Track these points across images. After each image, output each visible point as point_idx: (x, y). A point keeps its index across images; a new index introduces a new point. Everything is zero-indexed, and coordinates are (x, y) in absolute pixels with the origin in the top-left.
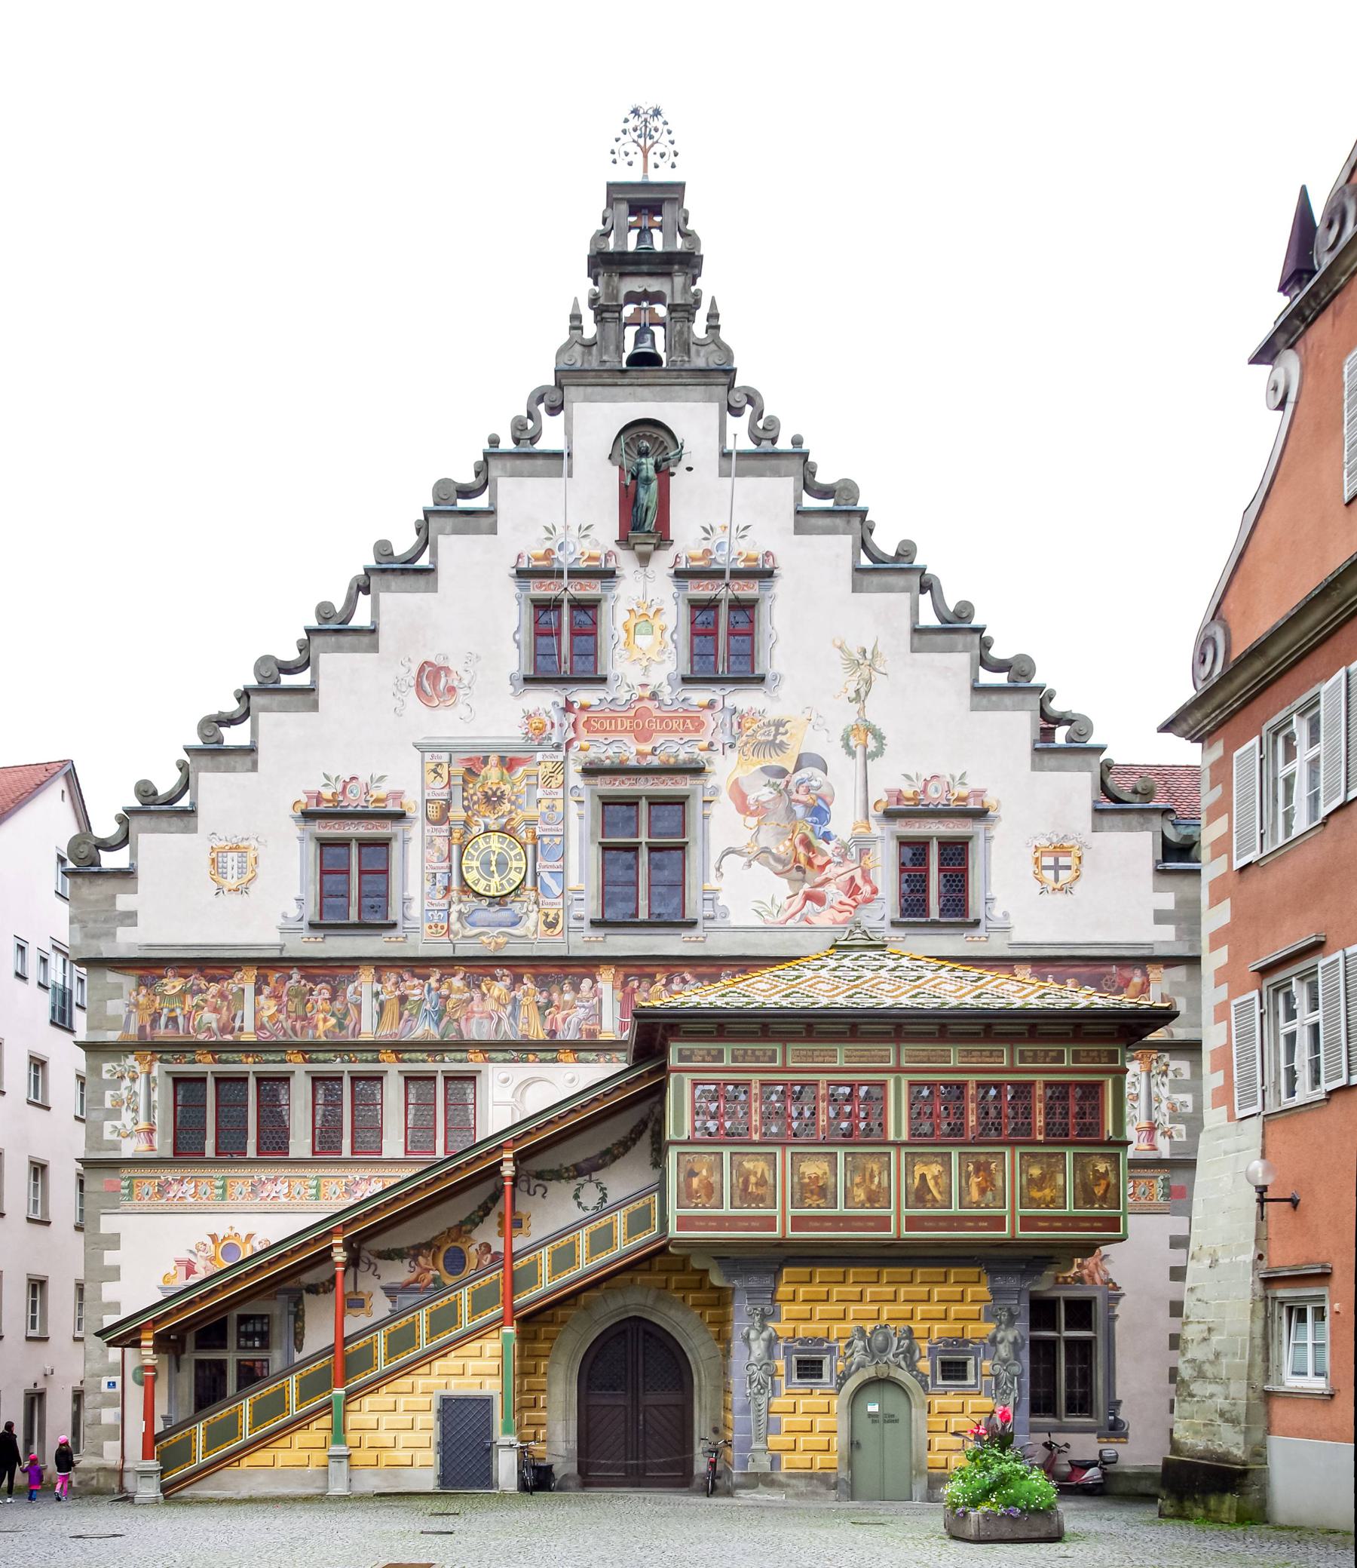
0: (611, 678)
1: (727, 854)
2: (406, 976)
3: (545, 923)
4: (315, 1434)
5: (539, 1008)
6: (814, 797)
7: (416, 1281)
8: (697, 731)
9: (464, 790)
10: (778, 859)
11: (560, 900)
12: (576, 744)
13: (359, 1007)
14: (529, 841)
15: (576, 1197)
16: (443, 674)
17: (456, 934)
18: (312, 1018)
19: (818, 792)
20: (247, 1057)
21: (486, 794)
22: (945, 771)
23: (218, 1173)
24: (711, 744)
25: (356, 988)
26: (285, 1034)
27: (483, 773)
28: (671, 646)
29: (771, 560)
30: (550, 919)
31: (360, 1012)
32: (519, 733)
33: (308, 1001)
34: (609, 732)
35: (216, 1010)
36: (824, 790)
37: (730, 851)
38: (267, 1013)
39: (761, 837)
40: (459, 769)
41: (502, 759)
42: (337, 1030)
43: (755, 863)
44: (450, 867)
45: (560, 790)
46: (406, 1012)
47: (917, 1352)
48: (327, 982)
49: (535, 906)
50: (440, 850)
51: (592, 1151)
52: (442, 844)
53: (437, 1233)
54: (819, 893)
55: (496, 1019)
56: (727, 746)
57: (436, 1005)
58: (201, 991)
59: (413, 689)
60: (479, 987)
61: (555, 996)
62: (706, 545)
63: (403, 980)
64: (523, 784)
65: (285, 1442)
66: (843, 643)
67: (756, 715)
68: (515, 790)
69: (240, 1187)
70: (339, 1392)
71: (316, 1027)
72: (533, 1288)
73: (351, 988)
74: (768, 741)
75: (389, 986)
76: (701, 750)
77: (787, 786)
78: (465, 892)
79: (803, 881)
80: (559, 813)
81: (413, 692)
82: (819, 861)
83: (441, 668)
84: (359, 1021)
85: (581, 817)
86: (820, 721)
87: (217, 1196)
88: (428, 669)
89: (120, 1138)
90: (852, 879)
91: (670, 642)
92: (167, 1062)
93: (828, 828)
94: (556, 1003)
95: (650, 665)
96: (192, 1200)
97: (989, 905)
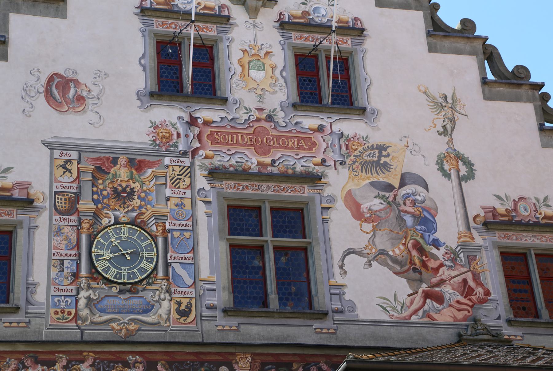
0: (230, 100)
1: (349, 254)
2: (28, 363)
3: (178, 311)
6: (419, 209)
8: (311, 149)
9: (93, 185)
10: (395, 261)
11: (192, 290)
12: (201, 152)
14: (160, 234)
16: (72, 86)
19: (423, 205)
21: (115, 190)
22: (530, 194)
24: (324, 161)
27: (112, 171)
28: (281, 81)
29: (359, 24)
30: (183, 307)
32: (147, 139)
34: (231, 144)
36: (428, 204)
37: (350, 252)
39: (377, 240)
40: (89, 167)
41: (131, 161)
43: (375, 264)
44: (79, 255)
45: (188, 192)
49: (167, 295)
50: (68, 238)
54: (436, 292)
56: (338, 163)
59: (42, 96)
62: (303, 8)
64: (152, 183)
66: (427, 89)
67: (360, 140)
68: (145, 188)
74: (373, 161)
76: (315, 165)
77: (395, 198)
78: (95, 280)
79: (421, 281)
80: (187, 210)
81: (42, 98)
82: (432, 264)
83: (72, 80)
85: (209, 215)
86: (417, 148)
88: (57, 80)
90: (465, 281)
91: (280, 78)
93: (437, 235)
95: (264, 94)
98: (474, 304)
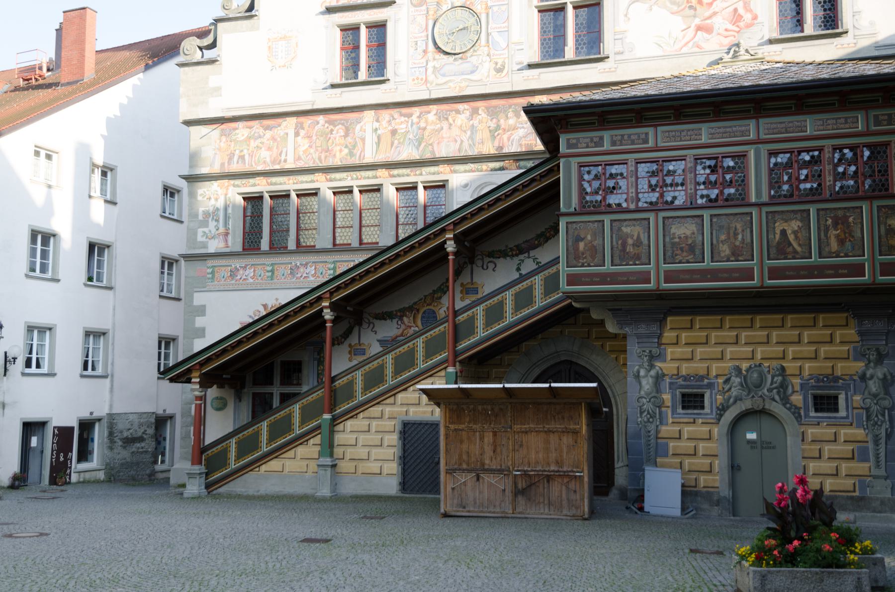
2: (396, 116)
4: (310, 449)
5: (490, 131)
7: (402, 335)
11: (506, 51)
13: (363, 140)
14: (483, 11)
15: (518, 269)
17: (431, 84)
18: (332, 150)
20: (289, 180)
23: (269, 260)
25: (361, 127)
26: (314, 163)
30: (499, 66)
31: (364, 144)
33: (330, 138)
35: (269, 149)
38: (302, 149)
42: (349, 157)
43: (655, 8)
44: (427, 35)
46: (396, 142)
47: (790, 387)
48: (343, 124)
51: (530, 236)
52: (421, 20)
53: (417, 300)
55: (459, 142)
57: (417, 135)
58: (260, 137)
60: (447, 119)
61: (502, 121)
63: (394, 119)
65: (291, 454)
69: (283, 271)
70: (327, 416)
71: (335, 155)
72: (471, 337)
73: (358, 127)
75: (384, 123)
79: (695, 16)
84: (363, 150)
87: (268, 277)
89: (207, 240)
90: (736, 10)
92: (238, 186)
94: (503, 126)
96: (251, 281)
97: (856, 17)
98: (741, 29)
